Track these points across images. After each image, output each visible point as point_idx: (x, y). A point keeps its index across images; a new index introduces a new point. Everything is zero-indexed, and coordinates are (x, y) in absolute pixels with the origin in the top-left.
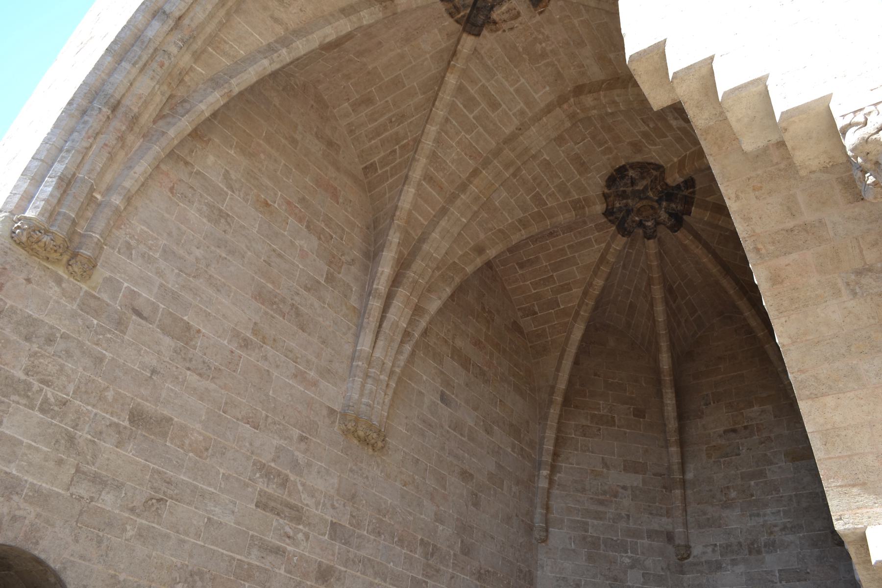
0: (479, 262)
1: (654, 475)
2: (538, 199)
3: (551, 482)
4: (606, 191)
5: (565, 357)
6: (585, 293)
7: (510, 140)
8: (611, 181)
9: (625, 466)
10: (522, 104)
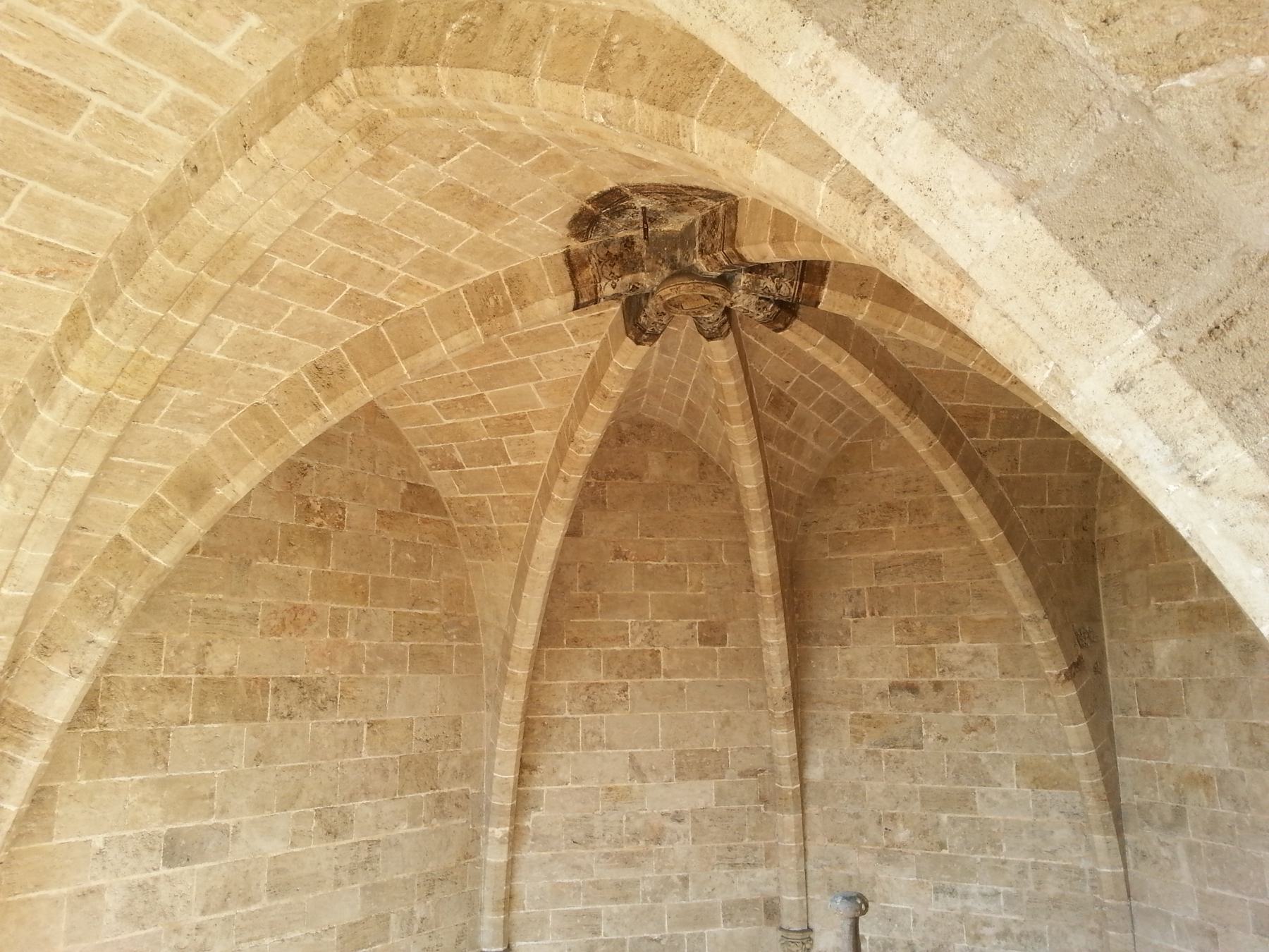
0: (195, 527)
1: (742, 775)
2: (355, 304)
3: (514, 839)
4: (576, 245)
5: (527, 585)
6: (560, 452)
7: (166, 210)
8: (583, 223)
9: (679, 766)
10: (172, 85)
